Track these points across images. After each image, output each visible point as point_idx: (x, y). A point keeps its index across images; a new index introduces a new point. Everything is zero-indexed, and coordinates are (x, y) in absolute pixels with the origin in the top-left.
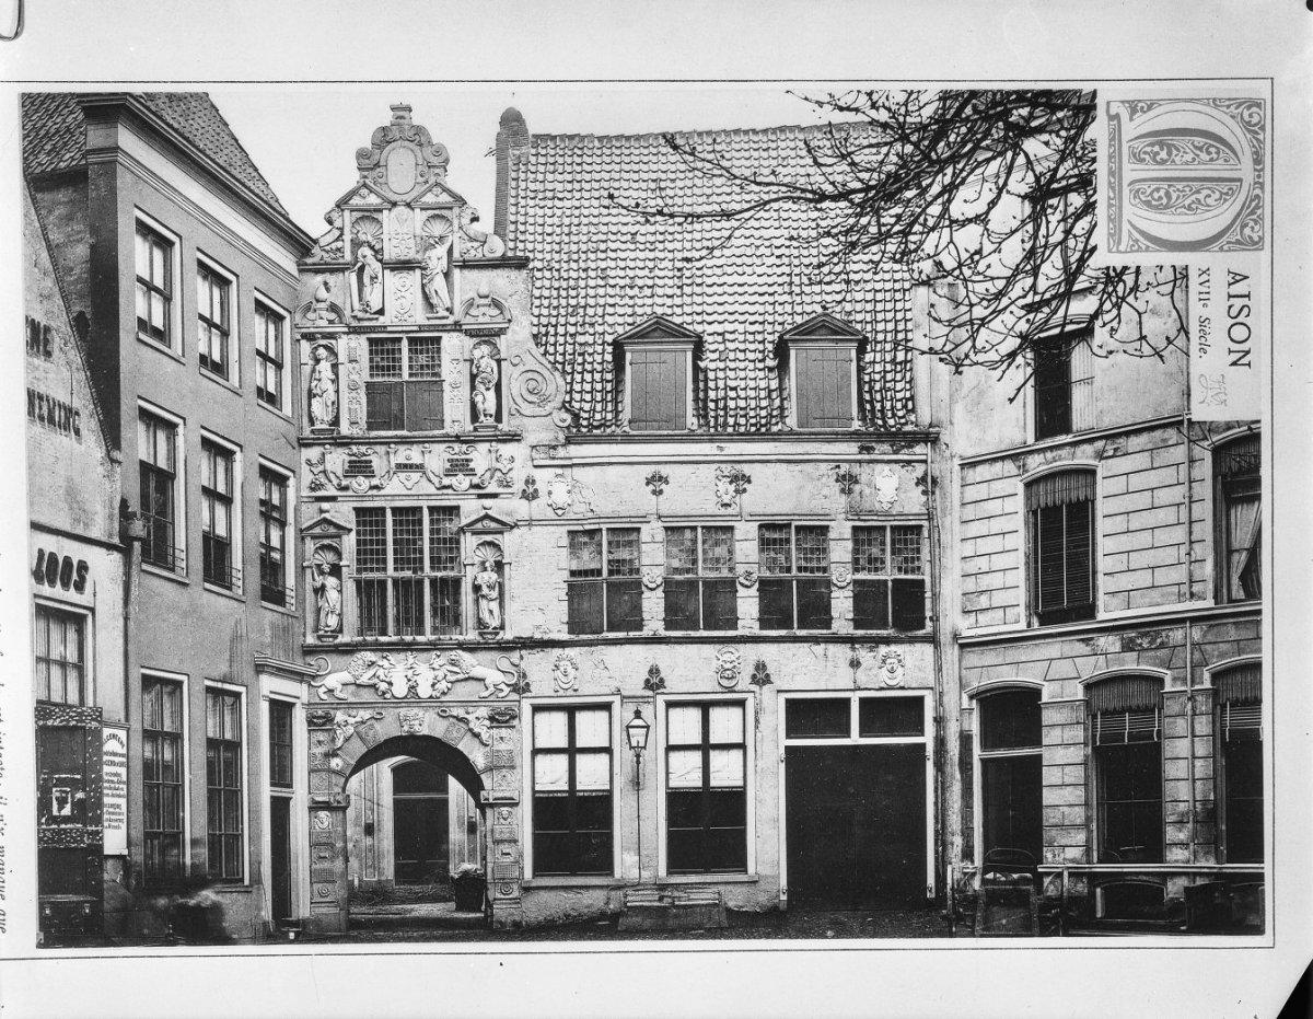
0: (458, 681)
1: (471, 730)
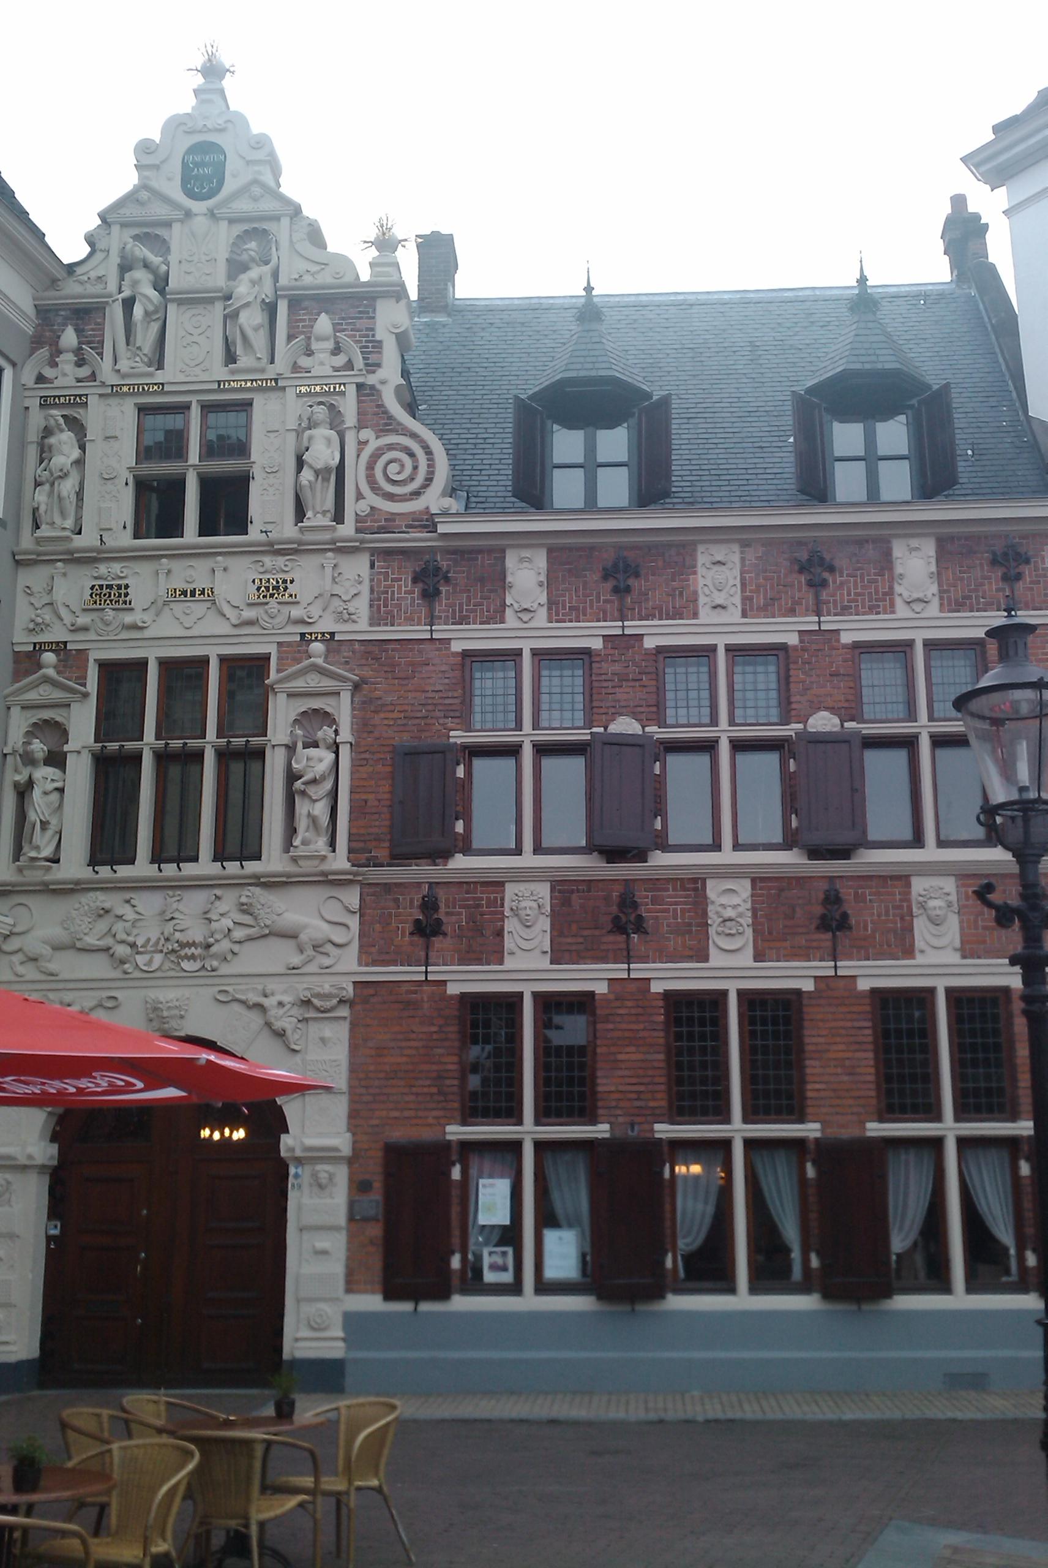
0: (251, 939)
1: (268, 1024)
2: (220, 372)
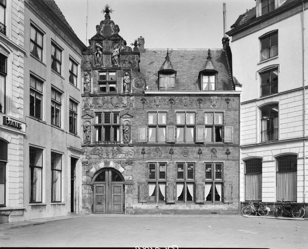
2: (111, 66)
